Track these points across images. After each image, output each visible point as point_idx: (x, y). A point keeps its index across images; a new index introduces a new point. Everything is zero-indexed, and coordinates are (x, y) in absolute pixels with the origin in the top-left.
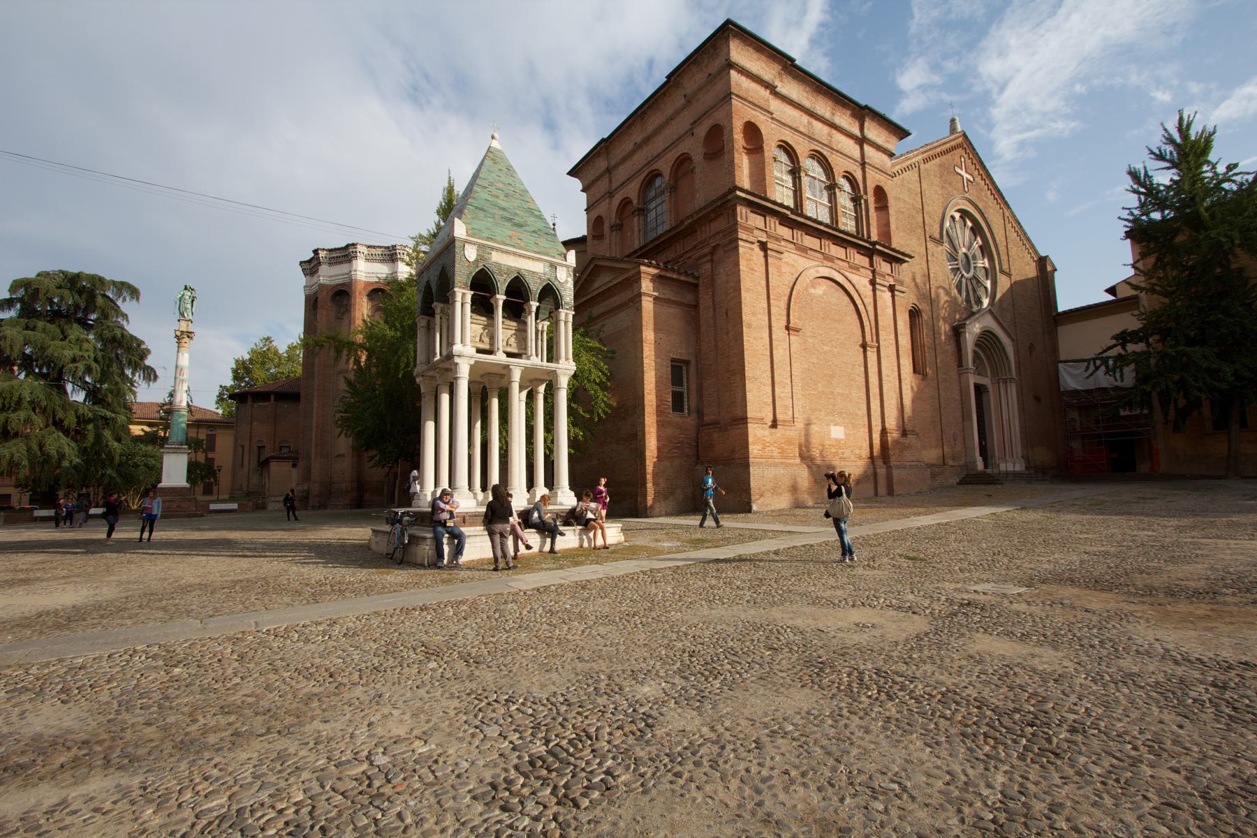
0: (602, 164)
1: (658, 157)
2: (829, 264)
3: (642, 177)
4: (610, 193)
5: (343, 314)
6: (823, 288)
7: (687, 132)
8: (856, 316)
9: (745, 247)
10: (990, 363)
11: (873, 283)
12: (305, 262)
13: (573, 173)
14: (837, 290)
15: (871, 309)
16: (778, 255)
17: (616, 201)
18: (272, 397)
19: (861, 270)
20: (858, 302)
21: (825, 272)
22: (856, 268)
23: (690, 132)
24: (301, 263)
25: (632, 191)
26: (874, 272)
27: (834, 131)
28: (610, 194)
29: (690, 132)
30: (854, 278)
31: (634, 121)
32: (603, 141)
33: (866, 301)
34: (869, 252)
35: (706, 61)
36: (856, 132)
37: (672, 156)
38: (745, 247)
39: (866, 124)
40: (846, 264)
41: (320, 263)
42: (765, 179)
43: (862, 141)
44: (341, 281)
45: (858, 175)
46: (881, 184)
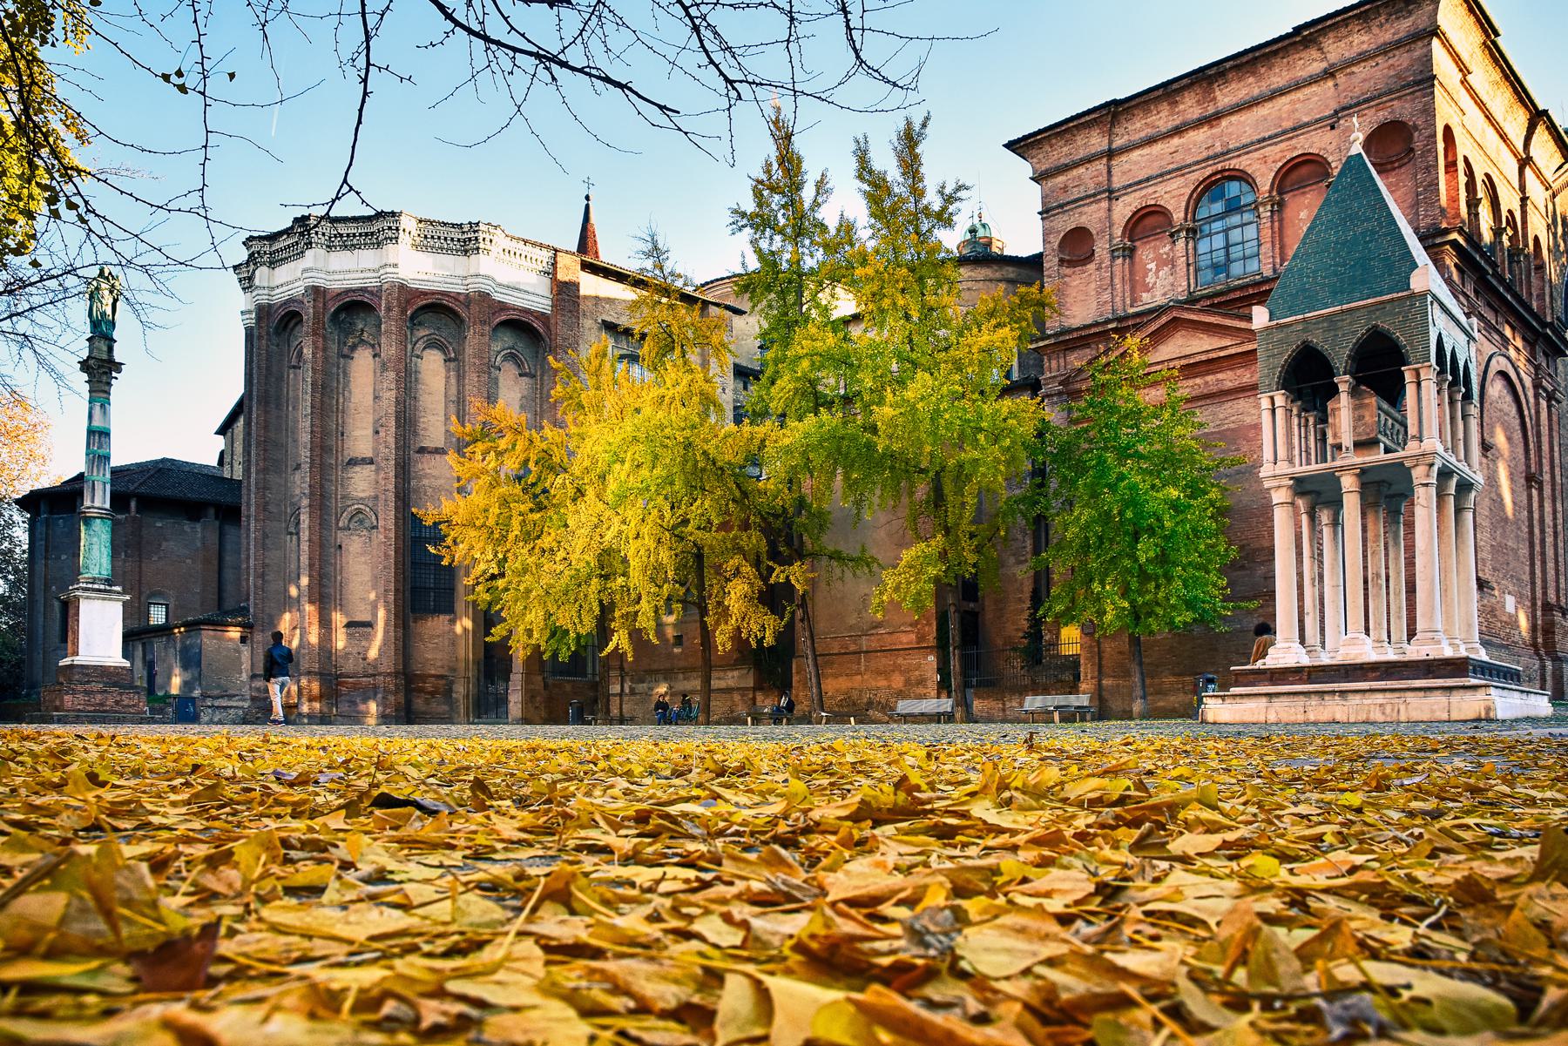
0: (1096, 141)
1: (1245, 149)
3: (1198, 175)
4: (1111, 191)
5: (354, 348)
7: (1317, 121)
12: (260, 238)
13: (1019, 146)
17: (1124, 209)
18: (133, 504)
23: (1332, 121)
24: (251, 238)
25: (1174, 196)
28: (1111, 194)
29: (1332, 121)
31: (1192, 84)
32: (1115, 102)
35: (1382, 19)
37: (1279, 154)
41: (309, 245)
44: (357, 284)
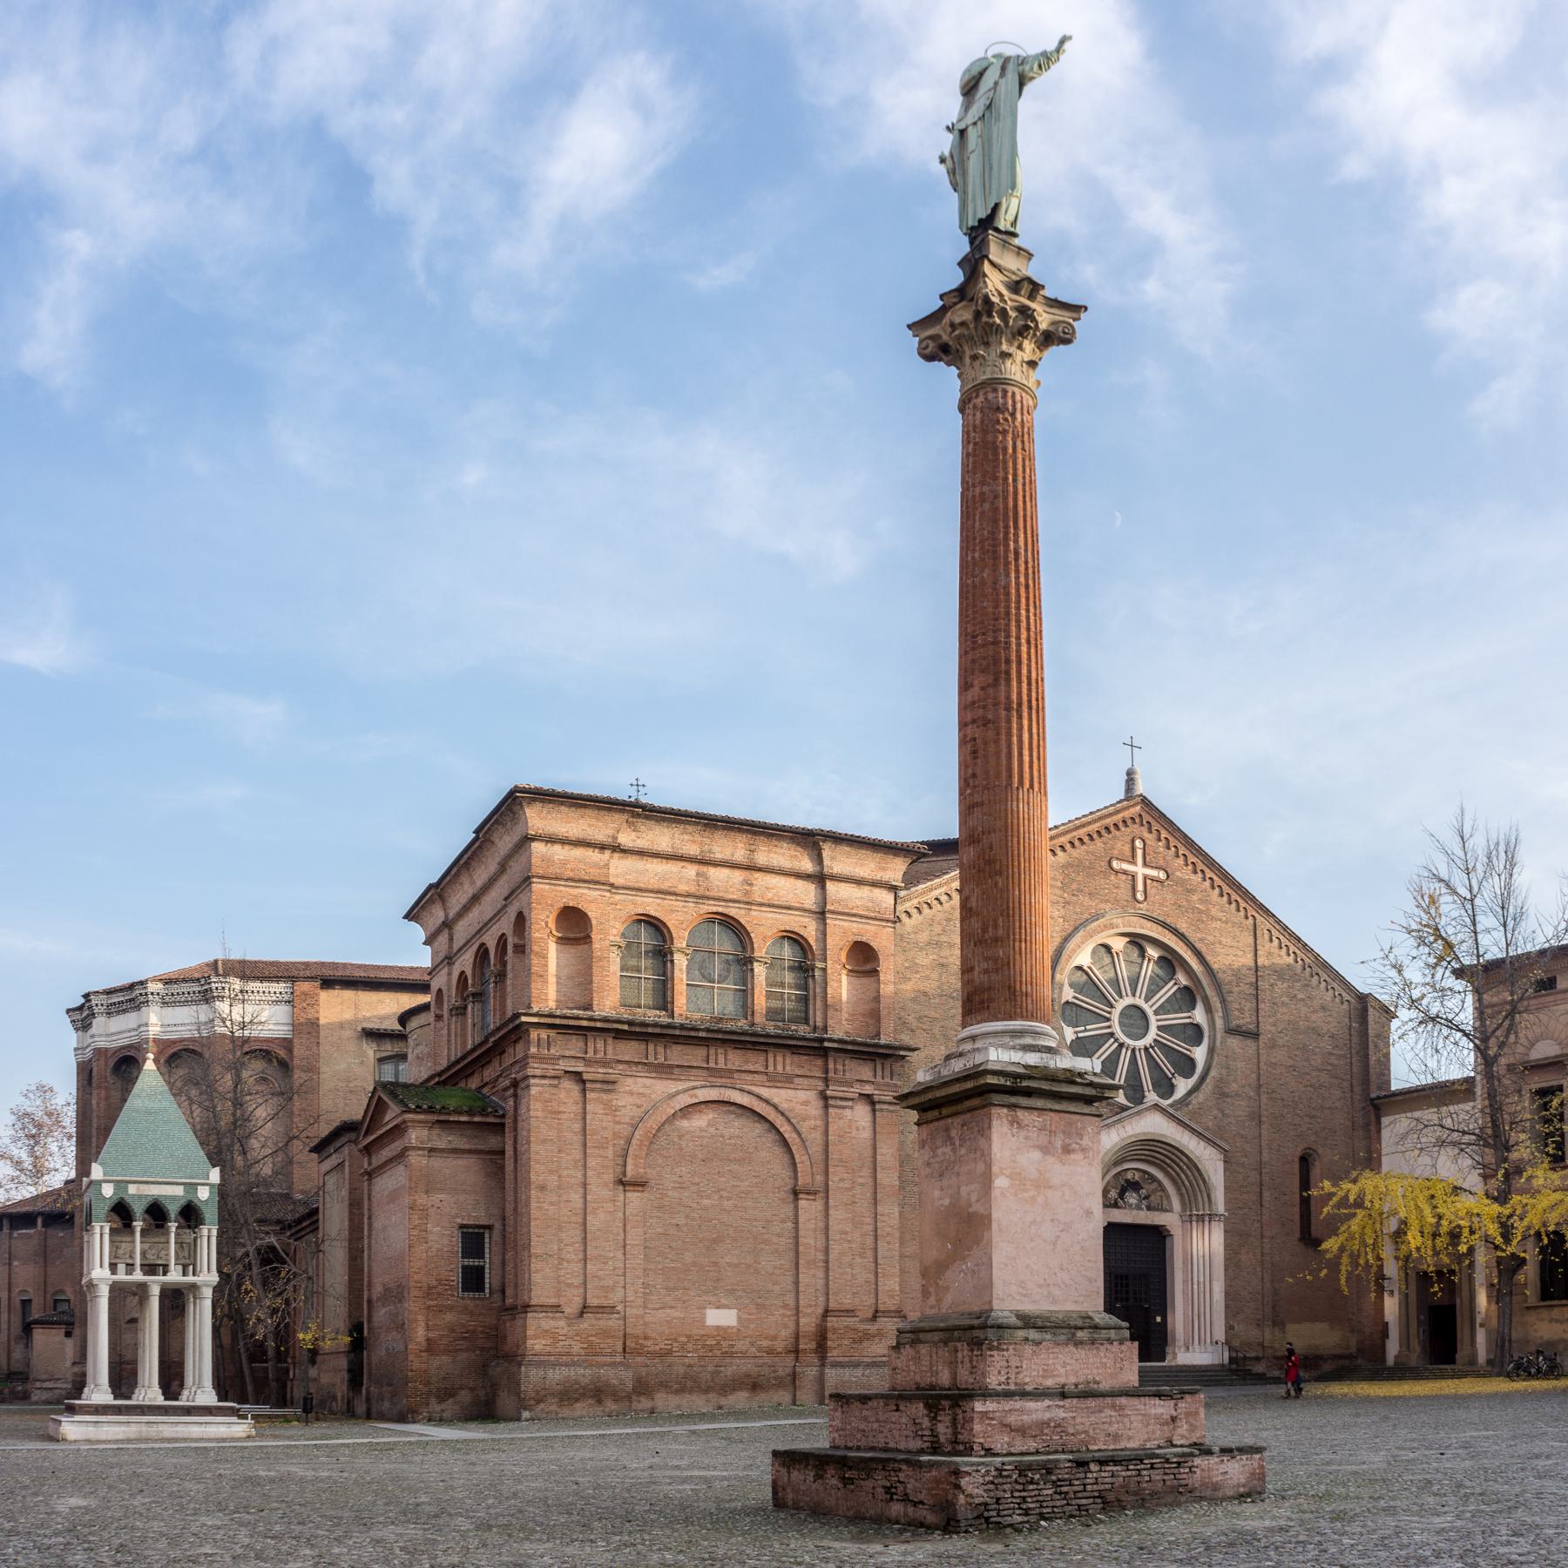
2: (719, 1081)
6: (699, 1121)
8: (778, 1150)
9: (537, 1085)
10: (1178, 1189)
11: (825, 1098)
14: (738, 1116)
15: (815, 1139)
16: (610, 1087)
19: (797, 1080)
20: (785, 1129)
21: (713, 1094)
22: (787, 1081)
26: (826, 1080)
27: (758, 875)
30: (779, 1096)
33: (804, 1128)
34: (818, 1049)
36: (807, 865)
38: (537, 1085)
39: (825, 854)
40: (764, 1078)
42: (591, 982)
43: (820, 879)
45: (810, 931)
46: (859, 939)
